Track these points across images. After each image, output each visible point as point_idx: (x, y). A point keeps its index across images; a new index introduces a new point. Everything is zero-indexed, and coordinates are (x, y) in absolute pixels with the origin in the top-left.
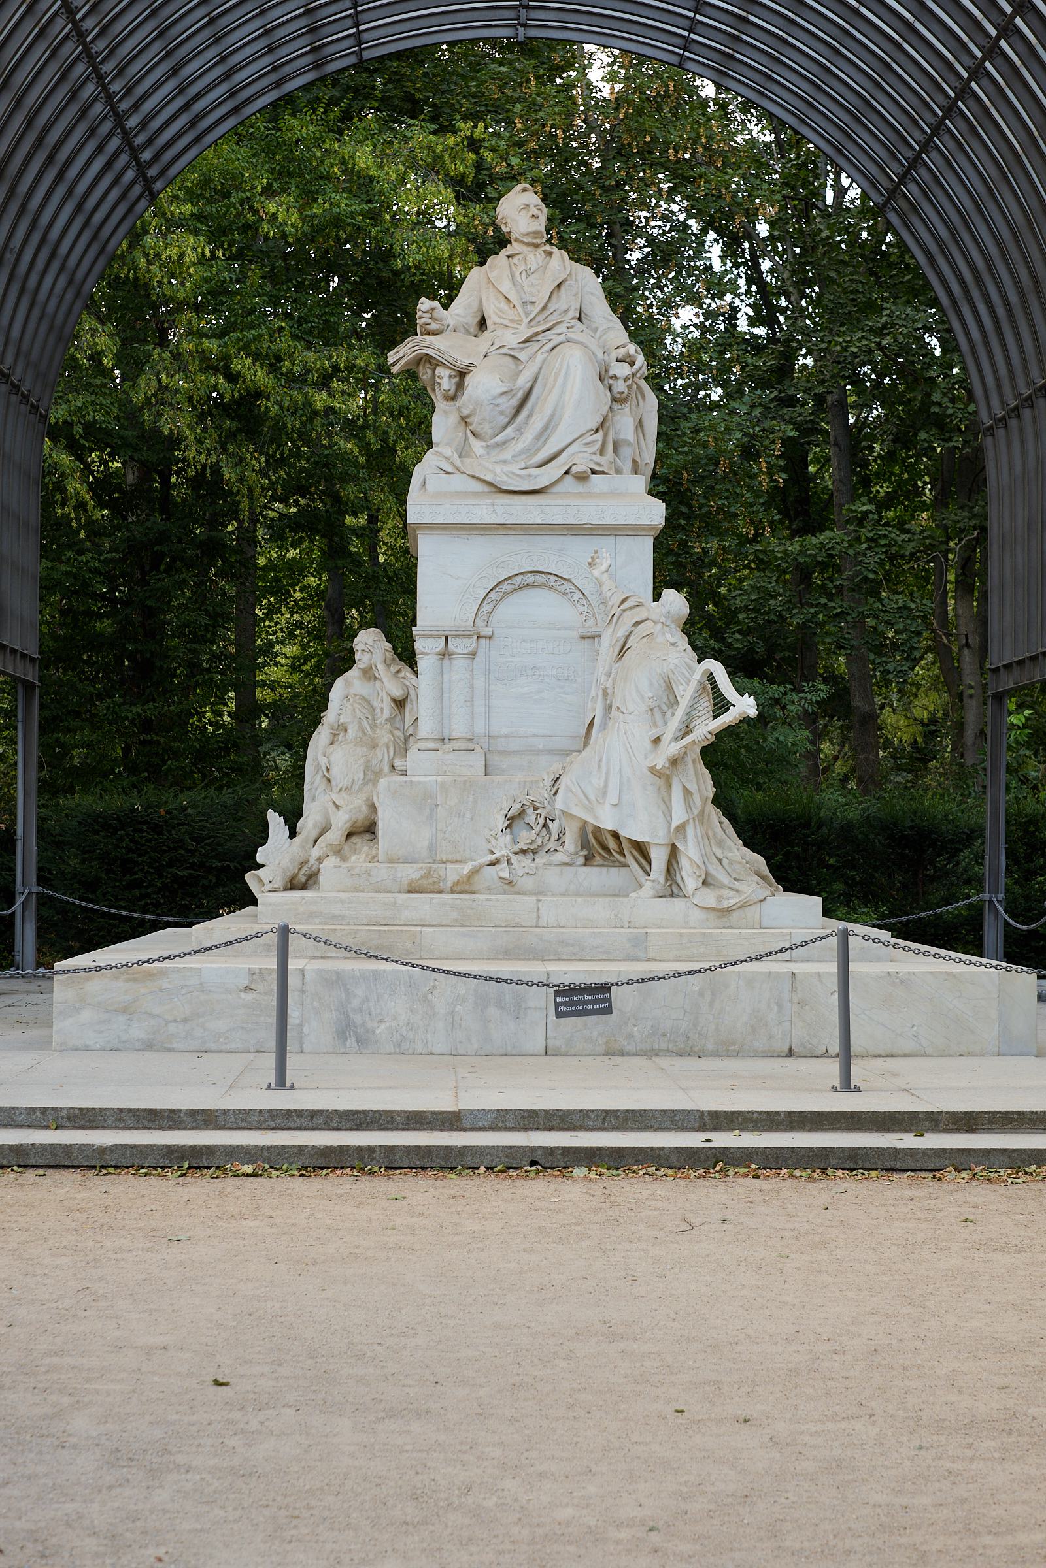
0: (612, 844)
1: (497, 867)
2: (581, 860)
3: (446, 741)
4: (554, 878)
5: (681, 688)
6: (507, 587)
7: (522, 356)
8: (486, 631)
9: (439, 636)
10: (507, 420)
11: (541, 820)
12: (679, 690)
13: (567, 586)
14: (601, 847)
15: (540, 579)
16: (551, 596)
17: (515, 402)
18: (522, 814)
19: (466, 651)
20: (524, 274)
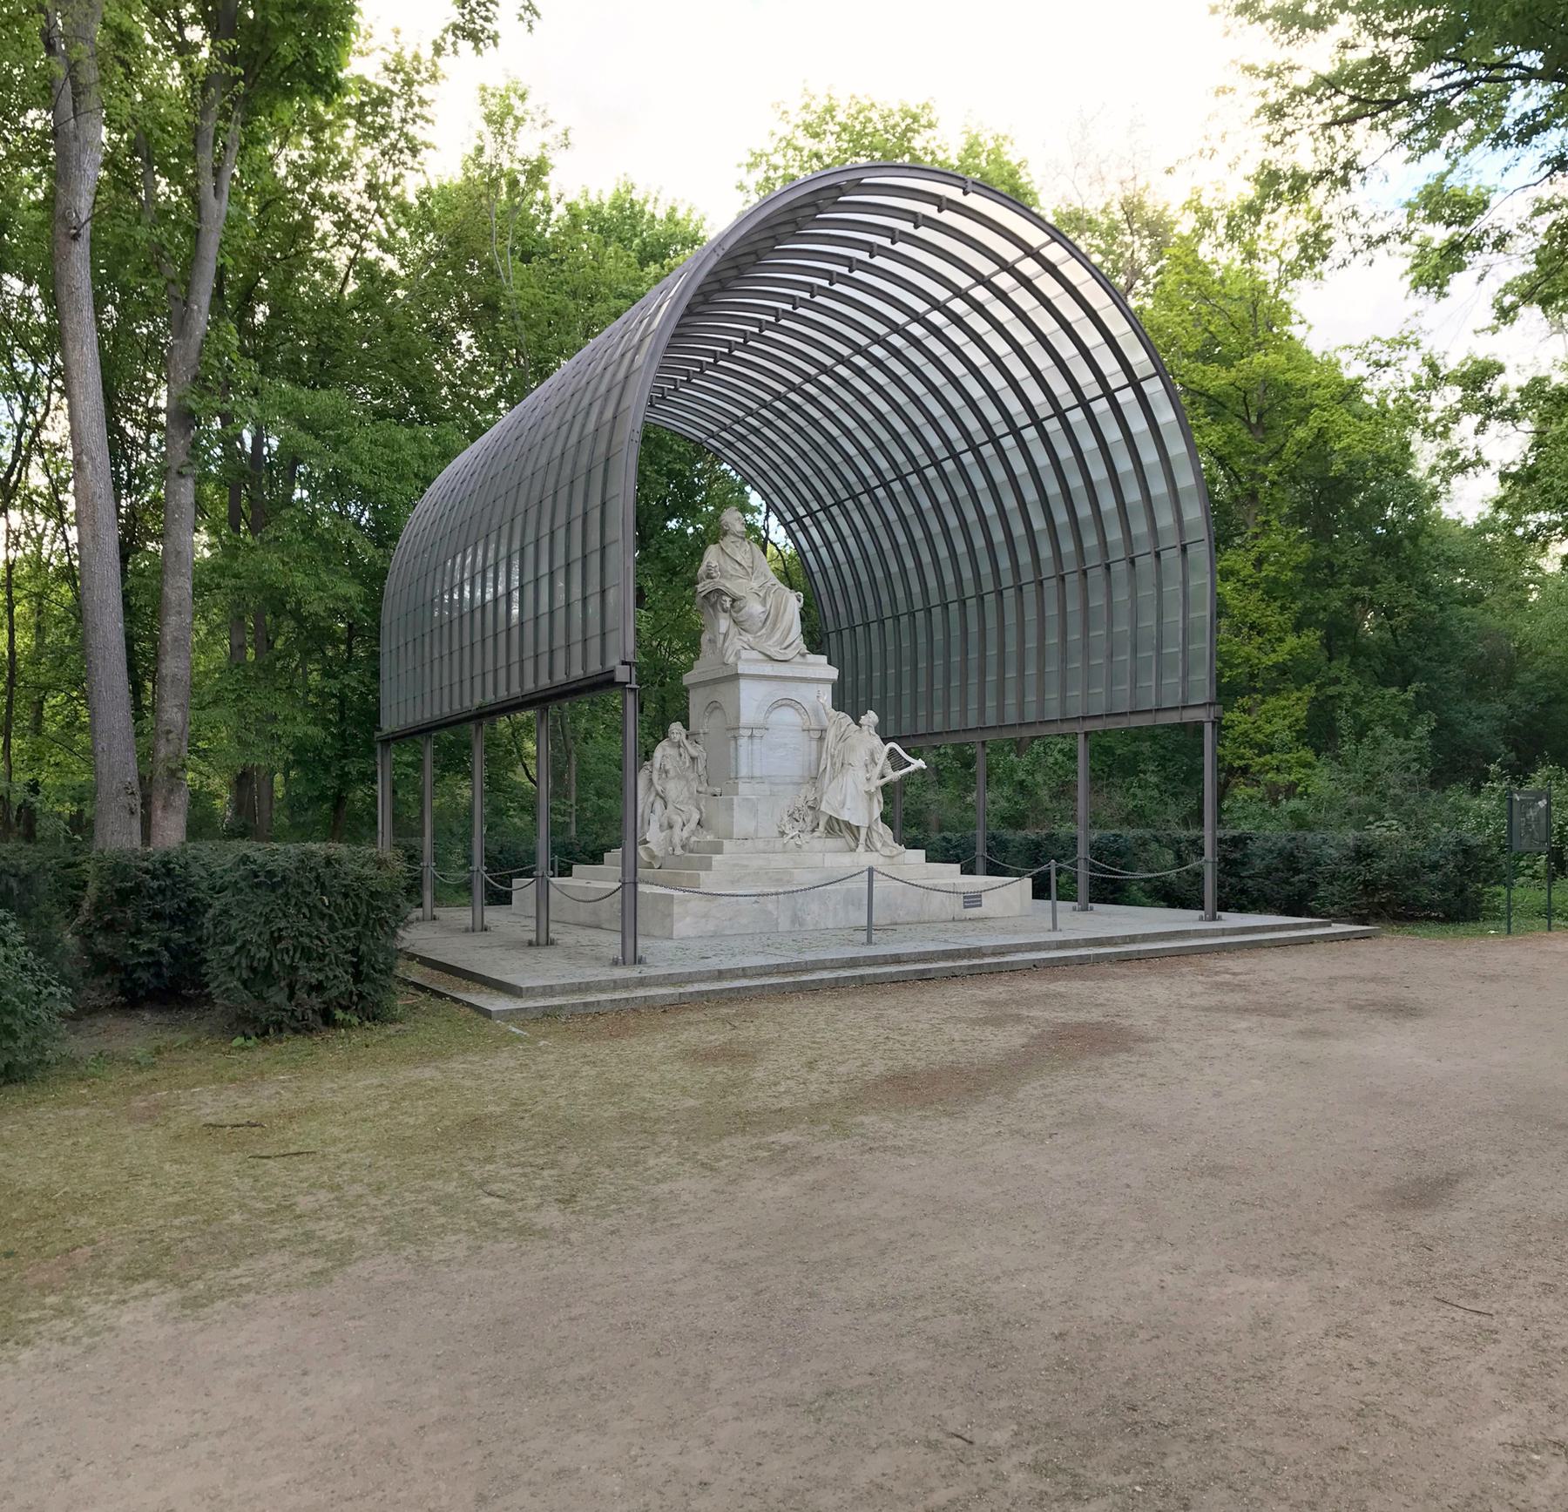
4: (818, 844)
14: (836, 827)
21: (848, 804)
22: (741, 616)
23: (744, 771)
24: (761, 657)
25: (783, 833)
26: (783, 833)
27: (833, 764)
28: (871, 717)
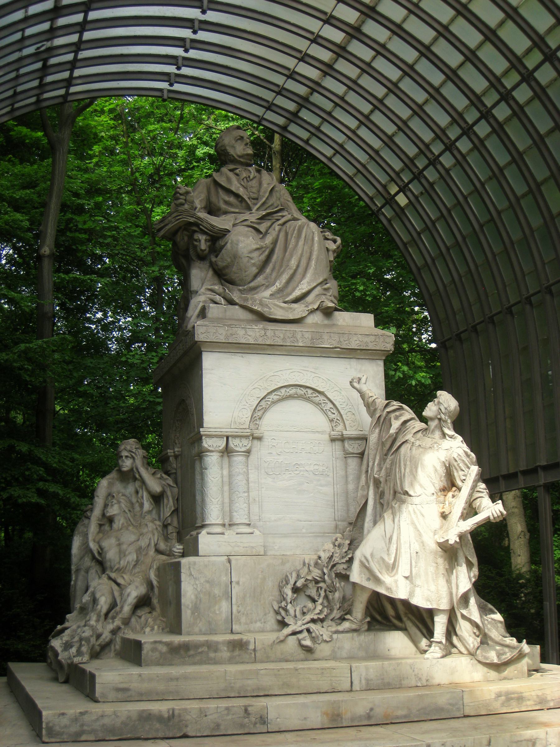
0: (391, 612)
1: (300, 636)
2: (366, 627)
3: (227, 526)
4: (348, 643)
5: (461, 473)
6: (273, 397)
7: (263, 227)
8: (257, 433)
9: (221, 437)
10: (257, 271)
11: (323, 593)
12: (458, 476)
13: (321, 398)
15: (301, 391)
16: (308, 407)
17: (263, 257)
19: (243, 449)
20: (245, 180)
22: (221, 261)
23: (213, 512)
24: (249, 316)
25: (283, 624)
26: (283, 624)
27: (381, 495)
28: (446, 402)
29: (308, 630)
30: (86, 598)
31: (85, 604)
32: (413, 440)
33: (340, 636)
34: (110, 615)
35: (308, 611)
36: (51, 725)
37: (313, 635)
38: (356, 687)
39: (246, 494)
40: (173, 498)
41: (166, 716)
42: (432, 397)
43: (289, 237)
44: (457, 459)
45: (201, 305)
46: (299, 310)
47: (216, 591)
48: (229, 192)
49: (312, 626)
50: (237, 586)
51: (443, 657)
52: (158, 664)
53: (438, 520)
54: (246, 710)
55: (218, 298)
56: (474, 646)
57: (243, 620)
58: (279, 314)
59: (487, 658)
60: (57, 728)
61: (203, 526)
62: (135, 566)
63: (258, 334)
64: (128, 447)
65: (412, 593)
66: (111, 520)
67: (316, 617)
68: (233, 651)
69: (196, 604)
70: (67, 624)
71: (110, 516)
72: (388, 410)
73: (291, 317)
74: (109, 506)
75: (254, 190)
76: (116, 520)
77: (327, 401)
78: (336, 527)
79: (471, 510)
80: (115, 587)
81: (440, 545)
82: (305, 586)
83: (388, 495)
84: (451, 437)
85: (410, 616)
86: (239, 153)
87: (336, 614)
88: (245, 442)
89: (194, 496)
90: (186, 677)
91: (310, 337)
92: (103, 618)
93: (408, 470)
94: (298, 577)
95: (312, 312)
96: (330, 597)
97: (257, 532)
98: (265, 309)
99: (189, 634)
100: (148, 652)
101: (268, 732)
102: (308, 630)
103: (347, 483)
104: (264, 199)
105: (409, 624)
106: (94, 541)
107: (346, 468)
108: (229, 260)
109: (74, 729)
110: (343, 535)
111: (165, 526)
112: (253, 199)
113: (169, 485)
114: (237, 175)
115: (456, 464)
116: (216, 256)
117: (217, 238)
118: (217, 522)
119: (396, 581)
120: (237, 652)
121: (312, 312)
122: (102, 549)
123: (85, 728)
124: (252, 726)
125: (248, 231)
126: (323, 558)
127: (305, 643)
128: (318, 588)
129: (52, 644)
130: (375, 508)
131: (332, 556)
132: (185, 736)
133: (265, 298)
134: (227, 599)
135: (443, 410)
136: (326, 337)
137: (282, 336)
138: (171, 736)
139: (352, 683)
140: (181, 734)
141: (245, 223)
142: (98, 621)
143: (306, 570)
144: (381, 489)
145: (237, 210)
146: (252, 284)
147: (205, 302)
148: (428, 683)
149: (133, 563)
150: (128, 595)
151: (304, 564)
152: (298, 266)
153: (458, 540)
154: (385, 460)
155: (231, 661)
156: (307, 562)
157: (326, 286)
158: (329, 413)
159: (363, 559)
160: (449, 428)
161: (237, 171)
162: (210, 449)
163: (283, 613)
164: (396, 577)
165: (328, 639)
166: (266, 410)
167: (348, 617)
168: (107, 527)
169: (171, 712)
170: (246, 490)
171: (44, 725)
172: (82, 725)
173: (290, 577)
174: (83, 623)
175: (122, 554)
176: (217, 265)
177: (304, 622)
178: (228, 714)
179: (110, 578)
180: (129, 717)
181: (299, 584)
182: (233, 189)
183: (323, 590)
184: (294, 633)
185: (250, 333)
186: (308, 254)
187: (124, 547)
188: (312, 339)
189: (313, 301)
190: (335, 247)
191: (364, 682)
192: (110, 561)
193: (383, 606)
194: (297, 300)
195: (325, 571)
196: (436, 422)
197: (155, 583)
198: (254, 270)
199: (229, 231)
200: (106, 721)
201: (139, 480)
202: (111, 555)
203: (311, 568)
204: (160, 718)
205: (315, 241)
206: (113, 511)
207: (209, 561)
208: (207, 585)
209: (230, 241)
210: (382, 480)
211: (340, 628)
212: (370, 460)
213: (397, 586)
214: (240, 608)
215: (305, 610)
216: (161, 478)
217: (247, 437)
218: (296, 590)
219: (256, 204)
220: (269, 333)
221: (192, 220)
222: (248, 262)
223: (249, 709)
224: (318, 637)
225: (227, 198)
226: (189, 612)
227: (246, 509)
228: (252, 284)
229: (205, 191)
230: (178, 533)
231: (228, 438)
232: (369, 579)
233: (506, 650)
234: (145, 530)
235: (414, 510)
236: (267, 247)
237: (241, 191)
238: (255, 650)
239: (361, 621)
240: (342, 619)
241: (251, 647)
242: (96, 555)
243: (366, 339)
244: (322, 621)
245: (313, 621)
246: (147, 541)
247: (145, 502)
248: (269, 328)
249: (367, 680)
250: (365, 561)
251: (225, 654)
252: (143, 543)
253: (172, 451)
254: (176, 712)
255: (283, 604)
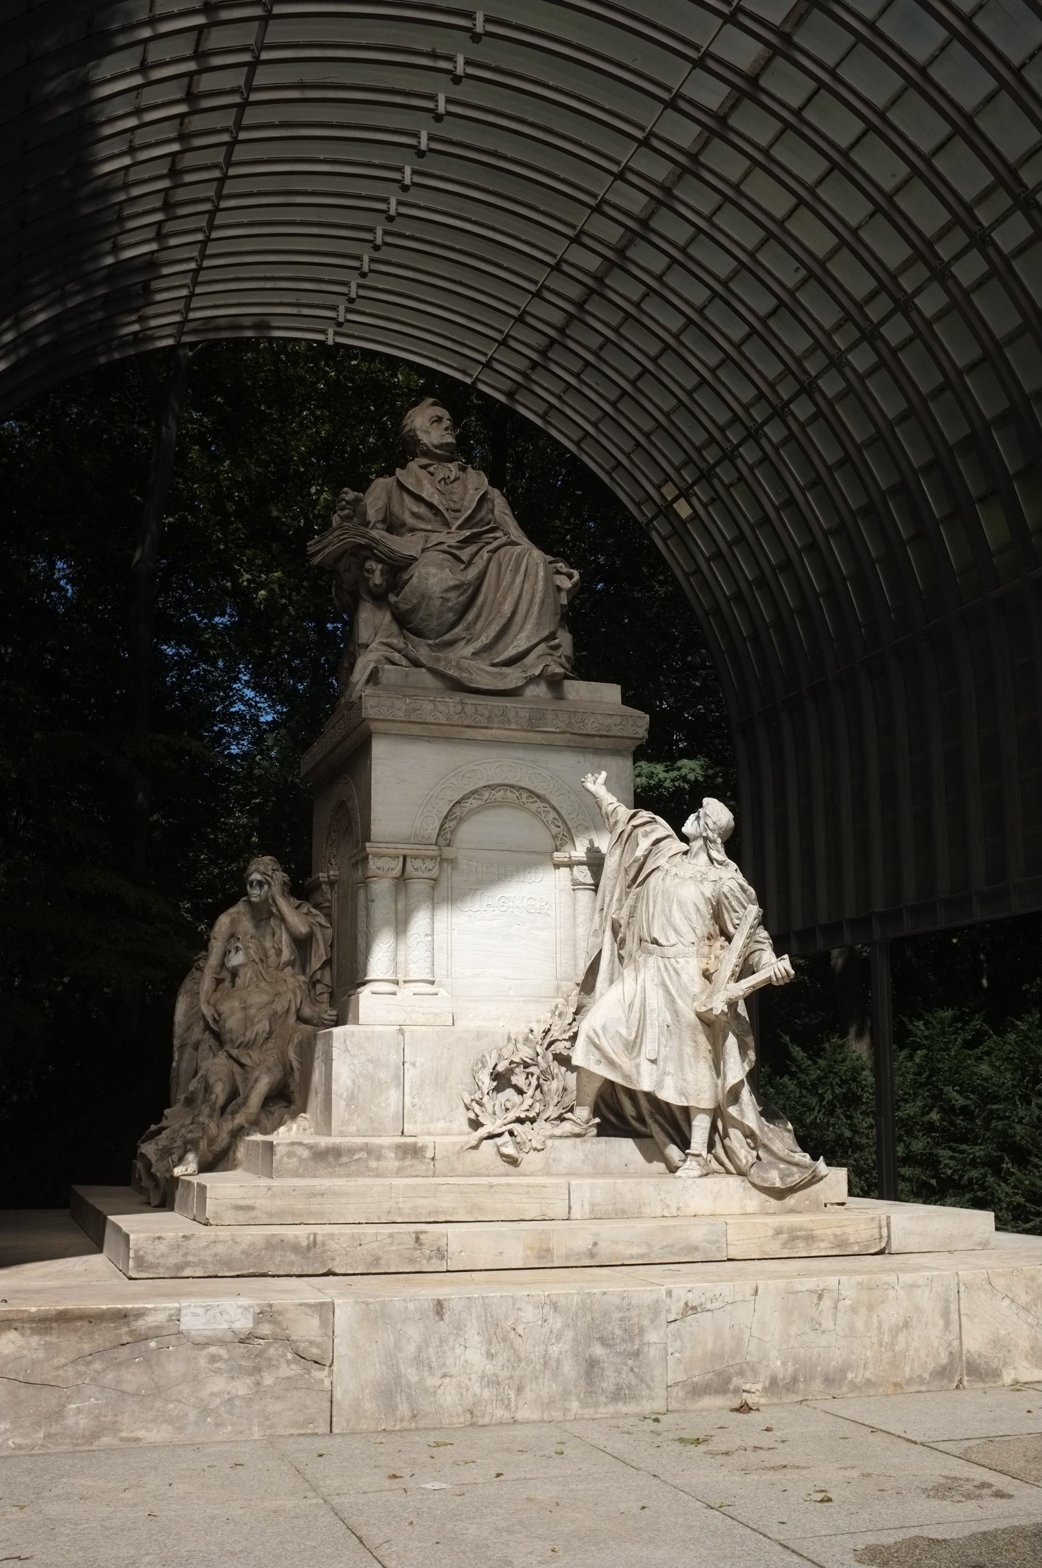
0: (629, 1110)
3: (401, 983)
5: (733, 915)
7: (465, 554)
10: (454, 618)
11: (534, 1083)
14: (624, 1114)
17: (463, 598)
18: (510, 1071)
19: (427, 875)
21: (649, 1049)
25: (475, 1124)
28: (716, 813)
29: (511, 1133)
30: (193, 1085)
31: (193, 1093)
32: (667, 866)
33: (557, 1142)
34: (229, 1109)
35: (513, 1107)
36: (141, 1253)
37: (518, 1139)
38: (576, 1213)
39: (430, 938)
40: (325, 943)
41: (305, 1244)
42: (695, 805)
43: (503, 569)
44: (729, 895)
45: (372, 666)
46: (513, 677)
47: (382, 1075)
48: (418, 499)
49: (517, 1128)
50: (411, 1069)
51: (701, 1176)
52: (296, 1174)
53: (699, 981)
54: (417, 1239)
55: (397, 656)
56: (747, 1162)
57: (420, 1116)
58: (484, 682)
59: (765, 1180)
60: (150, 1258)
61: (364, 984)
62: (267, 1039)
63: (452, 709)
64: (262, 868)
65: (660, 1083)
66: (234, 973)
67: (523, 1115)
68: (403, 1159)
69: (352, 1092)
70: (164, 1123)
71: (234, 967)
72: (635, 822)
73: (501, 686)
74: (233, 953)
75: (455, 498)
76: (241, 973)
77: (549, 809)
78: (558, 988)
79: (746, 969)
80: (236, 1068)
81: (700, 1016)
82: (510, 1071)
83: (631, 944)
84: (721, 863)
85: (658, 1117)
86: (436, 442)
87: (553, 1112)
88: (430, 864)
89: (356, 940)
90: (335, 1193)
91: (527, 715)
92: (217, 1113)
93: (658, 908)
94: (500, 1056)
95: (531, 680)
96: (545, 1088)
97: (442, 992)
98: (464, 675)
99: (342, 1134)
100: (282, 1157)
101: (448, 1271)
102: (511, 1133)
103: (575, 926)
104: (470, 512)
105: (655, 1130)
106: (208, 1003)
107: (574, 904)
108: (415, 601)
109: (174, 1259)
110: (567, 1001)
111: (313, 983)
112: (455, 511)
113: (321, 925)
114: (432, 474)
115: (726, 902)
116: (397, 595)
117: (398, 568)
118: (386, 977)
119: (638, 1066)
120: (408, 1162)
121: (531, 680)
122: (219, 1015)
123: (190, 1258)
124: (425, 1262)
125: (443, 559)
126: (535, 1032)
127: (505, 1150)
128: (528, 1074)
129: (143, 1151)
130: (612, 961)
131: (549, 1030)
132: (329, 1273)
133: (462, 658)
134: (397, 1086)
135: (711, 826)
136: (550, 716)
137: (487, 713)
138: (310, 1273)
139: (570, 1208)
140: (325, 1271)
141: (440, 547)
142: (211, 1116)
143: (511, 1046)
144: (620, 935)
145: (429, 527)
146: (447, 637)
147: (378, 661)
148: (679, 1213)
149: (265, 1035)
150: (256, 1080)
151: (509, 1039)
152: (514, 612)
153: (726, 1010)
154: (627, 894)
155: (399, 1172)
156: (513, 1037)
157: (553, 643)
158: (552, 826)
159: (591, 1034)
160: (718, 851)
161: (431, 469)
162: (380, 872)
163: (477, 1108)
164: (638, 1061)
165: (539, 1147)
166: (461, 820)
167: (569, 1115)
168: (227, 984)
169: (312, 1239)
170: (429, 932)
171: (132, 1254)
172: (186, 1254)
173: (488, 1058)
174: (188, 1121)
175: (248, 1021)
176: (397, 608)
177: (506, 1121)
178: (392, 1244)
179: (230, 1056)
180: (252, 1244)
181: (500, 1068)
182: (424, 495)
183: (535, 1077)
184: (491, 1137)
185: (441, 708)
186: (530, 596)
187: (253, 1011)
188: (530, 719)
189: (534, 665)
190: (570, 586)
191: (587, 1207)
192: (231, 1031)
193: (619, 1103)
194: (510, 662)
195: (539, 1050)
196: (700, 842)
197: (295, 1064)
198: (451, 616)
199: (416, 559)
200: (220, 1249)
201: (276, 917)
202: (232, 1023)
203: (518, 1046)
204: (296, 1248)
205: (540, 578)
206: (236, 959)
207: (373, 1032)
208: (370, 1066)
209: (416, 574)
210: (622, 922)
211: (558, 1131)
212: (607, 893)
213: (639, 1073)
214: (416, 1101)
215: (509, 1105)
216: (308, 913)
217: (432, 858)
218: (496, 1076)
219: (457, 519)
220: (469, 709)
221: (363, 541)
222: (442, 604)
223: (422, 1237)
224: (524, 1142)
225: (415, 509)
226: (343, 1103)
227: (429, 959)
228: (447, 637)
229: (384, 496)
230: (331, 994)
231: (405, 857)
232: (599, 1062)
233: (794, 1169)
234: (282, 989)
235: (665, 965)
236: (470, 584)
237: (435, 500)
238: (433, 1159)
239: (587, 1122)
240: (561, 1119)
241: (429, 1154)
242: (211, 1022)
243: (609, 721)
244: (533, 1121)
245: (520, 1121)
246: (286, 1004)
247: (284, 948)
248: (469, 701)
249: (592, 1205)
250: (594, 1036)
251: (391, 1162)
252: (279, 1007)
253: (325, 875)
254: (319, 1239)
255: (477, 1096)
